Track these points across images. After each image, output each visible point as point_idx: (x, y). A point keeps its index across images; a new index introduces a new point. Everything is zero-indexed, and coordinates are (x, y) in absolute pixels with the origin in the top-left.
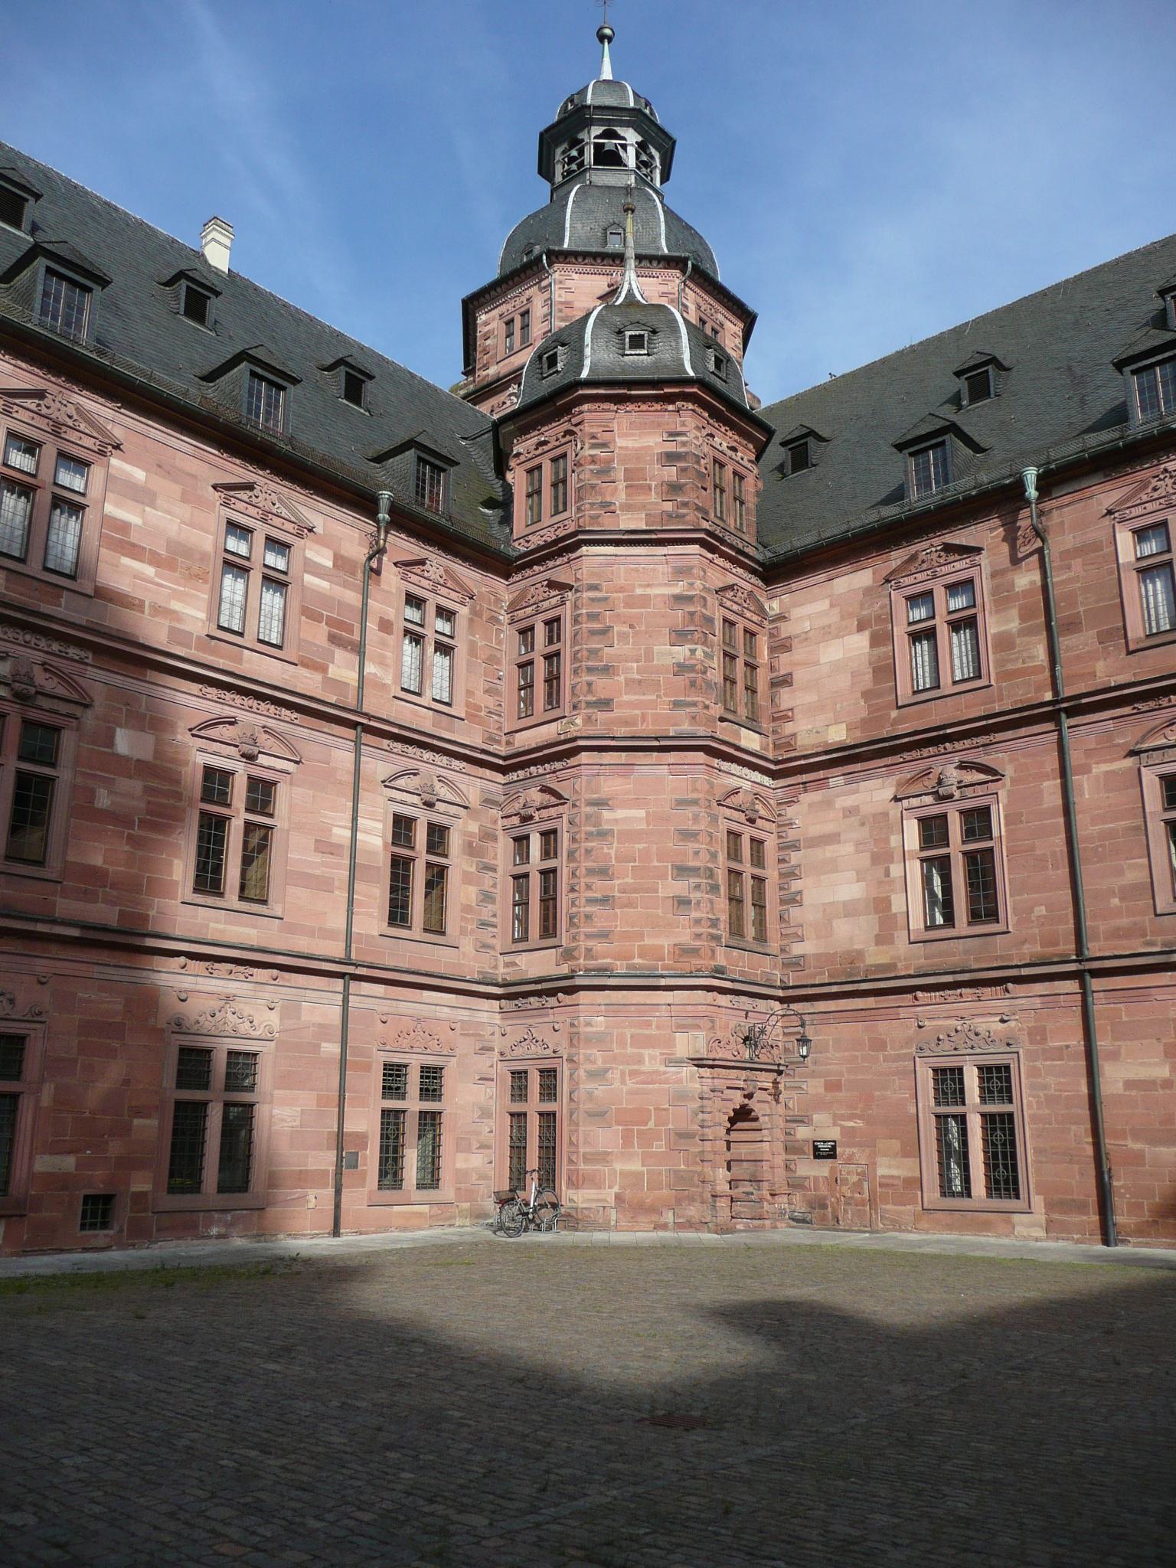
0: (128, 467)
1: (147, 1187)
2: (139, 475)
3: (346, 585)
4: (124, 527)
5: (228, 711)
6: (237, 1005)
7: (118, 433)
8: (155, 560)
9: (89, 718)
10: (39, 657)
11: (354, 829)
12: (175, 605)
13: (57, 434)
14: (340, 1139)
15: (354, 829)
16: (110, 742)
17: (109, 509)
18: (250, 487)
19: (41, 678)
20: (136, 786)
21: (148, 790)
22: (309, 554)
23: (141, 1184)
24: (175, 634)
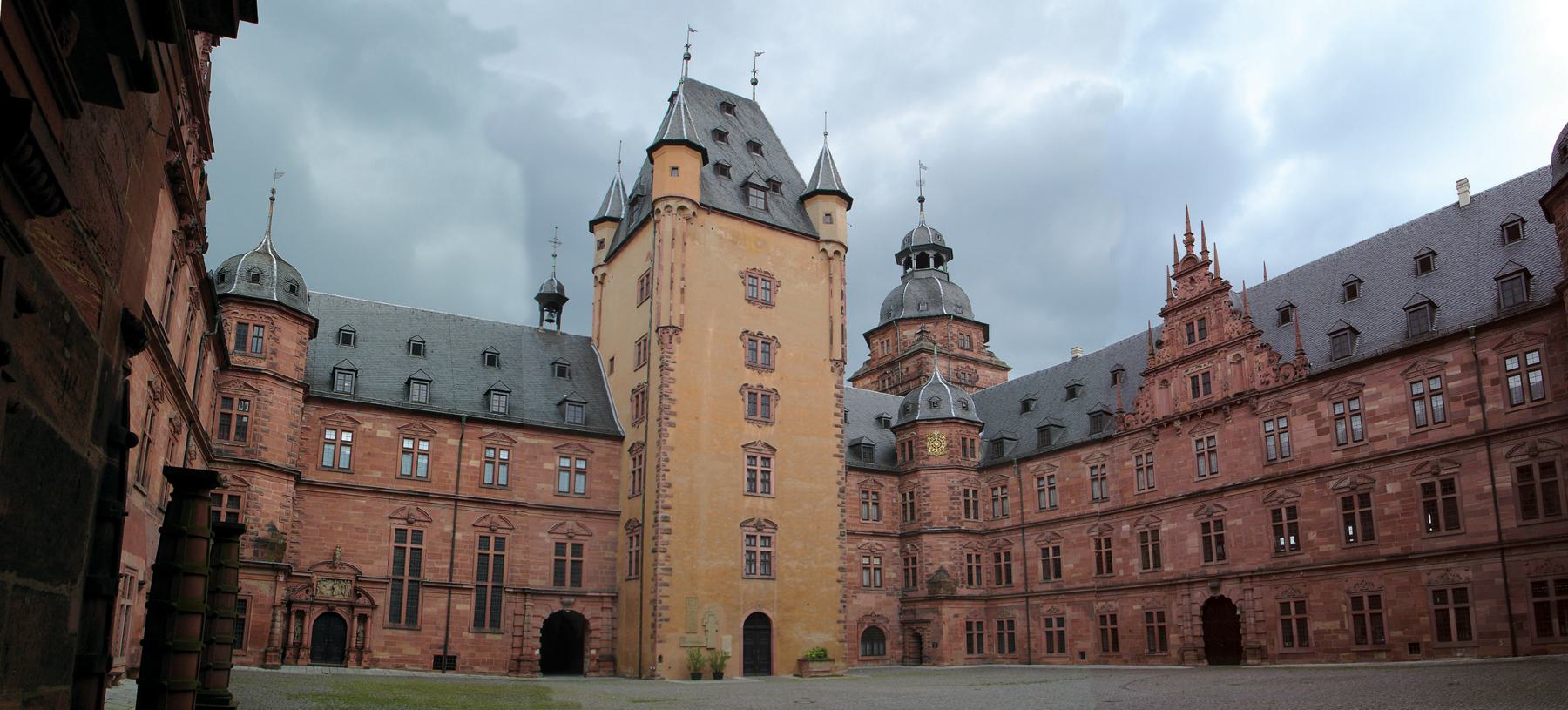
0: (1369, 390)
1: (1429, 640)
2: (1374, 389)
3: (1469, 376)
4: (1373, 412)
5: (1425, 460)
6: (1452, 572)
7: (1363, 380)
8: (1387, 417)
9: (1377, 486)
10: (1357, 473)
11: (1493, 482)
12: (1397, 429)
13: (1345, 395)
14: (1511, 618)
15: (1493, 482)
16: (1385, 490)
17: (1367, 409)
18: (1415, 364)
19: (1360, 481)
20: (1397, 502)
21: (1402, 502)
22: (1448, 374)
23: (1427, 639)
24: (1400, 441)
